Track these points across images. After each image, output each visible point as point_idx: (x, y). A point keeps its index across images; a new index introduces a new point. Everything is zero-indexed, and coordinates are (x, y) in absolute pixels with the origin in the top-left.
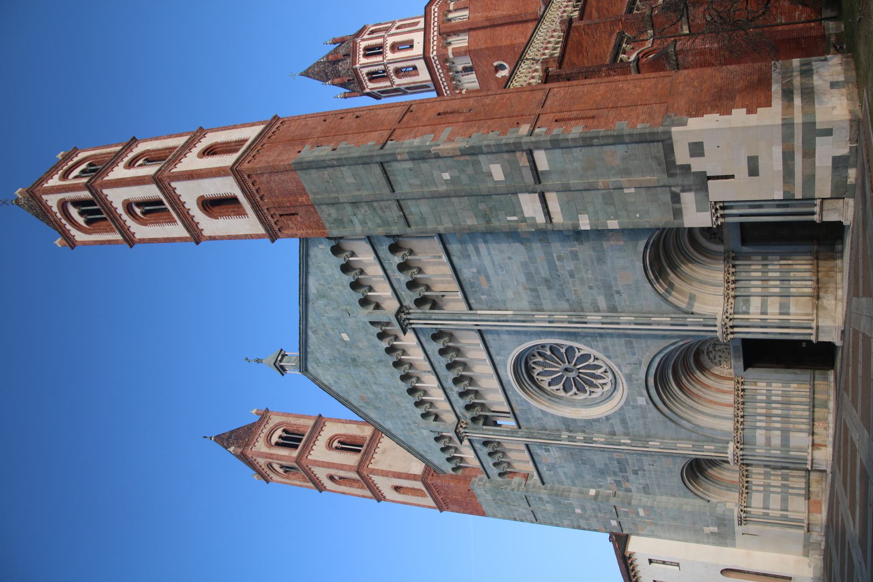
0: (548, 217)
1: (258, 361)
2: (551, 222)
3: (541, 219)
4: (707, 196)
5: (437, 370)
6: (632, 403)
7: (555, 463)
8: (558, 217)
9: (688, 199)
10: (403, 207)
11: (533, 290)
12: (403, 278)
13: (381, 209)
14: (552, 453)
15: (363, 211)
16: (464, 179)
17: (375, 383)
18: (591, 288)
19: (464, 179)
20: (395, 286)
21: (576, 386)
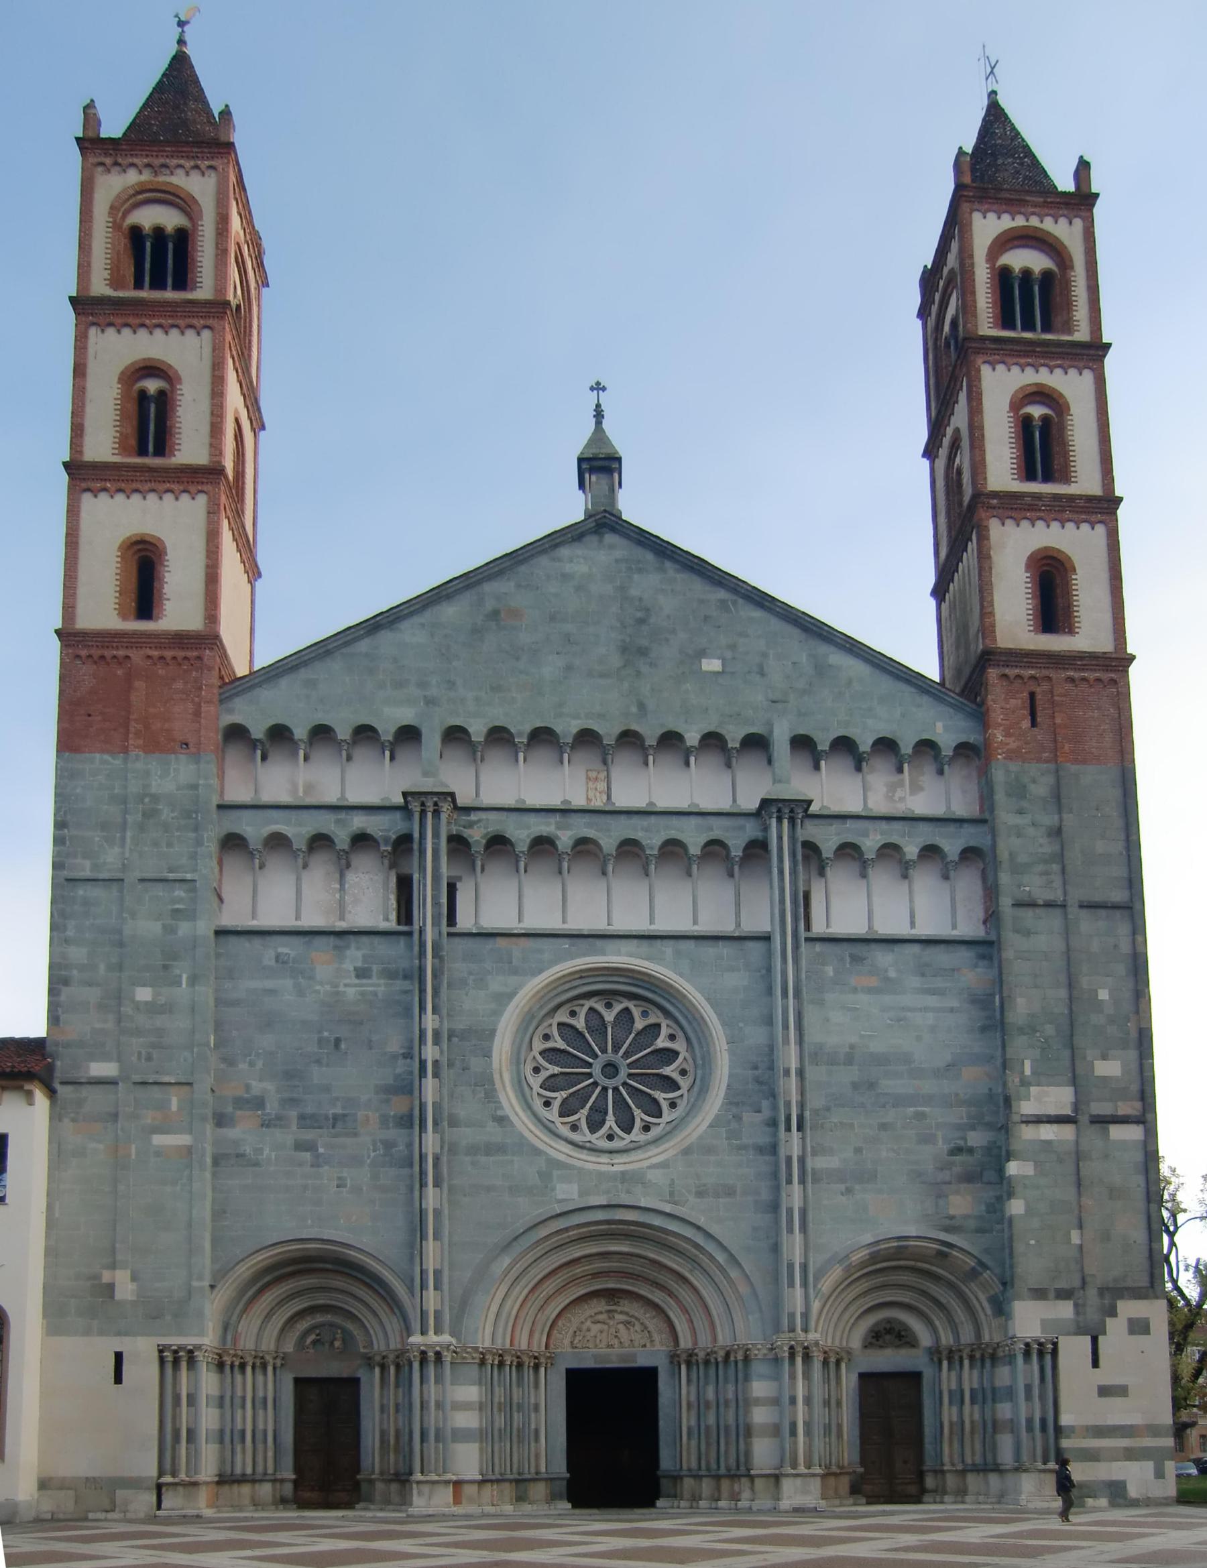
0: (1034, 1119)
1: (599, 414)
2: (1027, 1122)
3: (1027, 1108)
4: (1068, 1334)
5: (623, 817)
6: (556, 1173)
7: (311, 978)
8: (1028, 1133)
9: (1065, 1310)
10: (1050, 909)
11: (849, 1060)
12: (871, 843)
13: (1046, 873)
14: (357, 981)
15: (1041, 841)
16: (1097, 1019)
17: (569, 668)
18: (858, 1150)
19: (1097, 1019)
20: (849, 822)
21: (562, 1073)
